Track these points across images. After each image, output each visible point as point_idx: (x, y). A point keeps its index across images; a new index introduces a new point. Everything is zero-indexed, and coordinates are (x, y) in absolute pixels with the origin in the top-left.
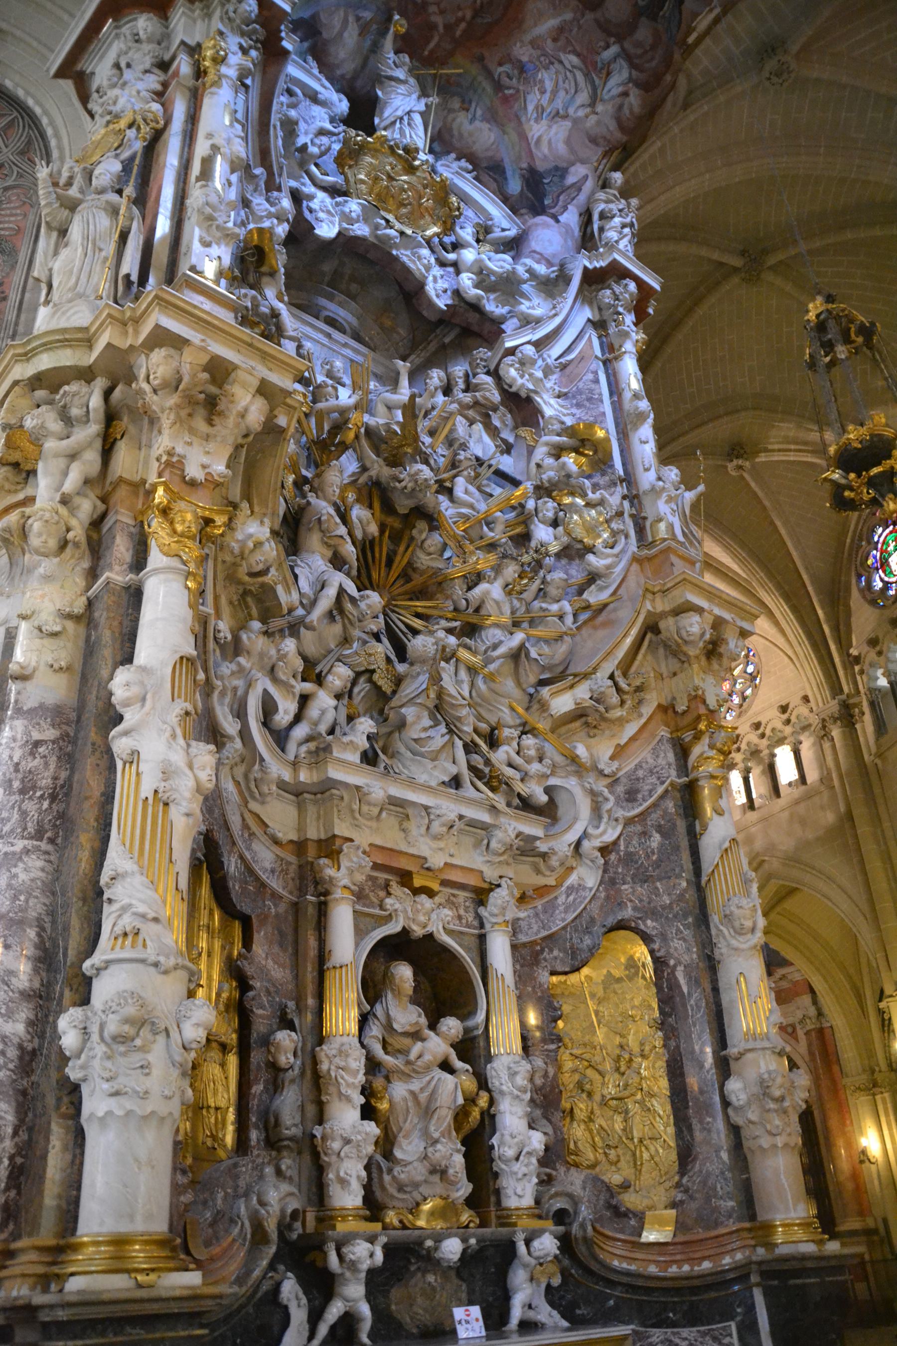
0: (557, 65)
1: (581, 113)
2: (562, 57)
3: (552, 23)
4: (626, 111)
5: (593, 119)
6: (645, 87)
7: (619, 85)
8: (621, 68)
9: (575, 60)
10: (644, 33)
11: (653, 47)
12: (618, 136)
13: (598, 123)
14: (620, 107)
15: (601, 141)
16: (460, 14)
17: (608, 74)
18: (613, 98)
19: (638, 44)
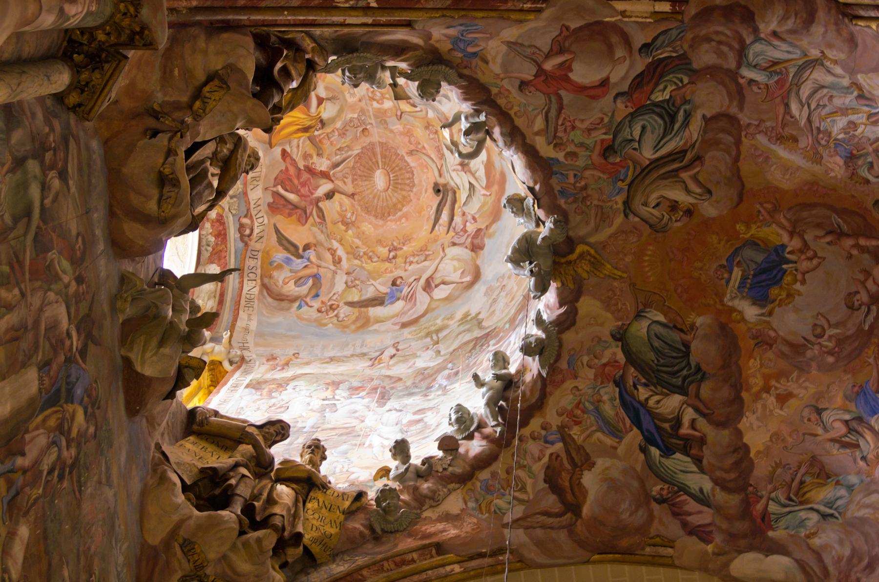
0: (816, 124)
1: (838, 70)
2: (803, 122)
3: (782, 152)
4: (790, 24)
5: (831, 54)
6: (748, 17)
7: (774, 47)
8: (757, 55)
9: (794, 107)
10: (704, 57)
11: (708, 39)
12: (821, 14)
13: (830, 46)
14: (792, 32)
15: (845, 33)
16: (855, 252)
17: (775, 63)
18: (791, 44)
19: (720, 54)
